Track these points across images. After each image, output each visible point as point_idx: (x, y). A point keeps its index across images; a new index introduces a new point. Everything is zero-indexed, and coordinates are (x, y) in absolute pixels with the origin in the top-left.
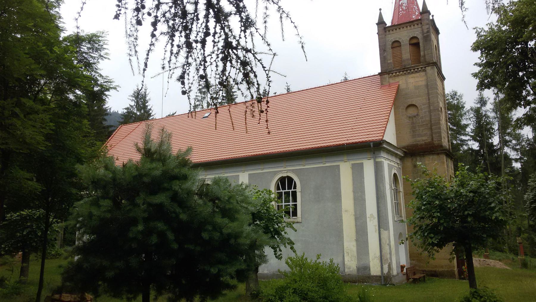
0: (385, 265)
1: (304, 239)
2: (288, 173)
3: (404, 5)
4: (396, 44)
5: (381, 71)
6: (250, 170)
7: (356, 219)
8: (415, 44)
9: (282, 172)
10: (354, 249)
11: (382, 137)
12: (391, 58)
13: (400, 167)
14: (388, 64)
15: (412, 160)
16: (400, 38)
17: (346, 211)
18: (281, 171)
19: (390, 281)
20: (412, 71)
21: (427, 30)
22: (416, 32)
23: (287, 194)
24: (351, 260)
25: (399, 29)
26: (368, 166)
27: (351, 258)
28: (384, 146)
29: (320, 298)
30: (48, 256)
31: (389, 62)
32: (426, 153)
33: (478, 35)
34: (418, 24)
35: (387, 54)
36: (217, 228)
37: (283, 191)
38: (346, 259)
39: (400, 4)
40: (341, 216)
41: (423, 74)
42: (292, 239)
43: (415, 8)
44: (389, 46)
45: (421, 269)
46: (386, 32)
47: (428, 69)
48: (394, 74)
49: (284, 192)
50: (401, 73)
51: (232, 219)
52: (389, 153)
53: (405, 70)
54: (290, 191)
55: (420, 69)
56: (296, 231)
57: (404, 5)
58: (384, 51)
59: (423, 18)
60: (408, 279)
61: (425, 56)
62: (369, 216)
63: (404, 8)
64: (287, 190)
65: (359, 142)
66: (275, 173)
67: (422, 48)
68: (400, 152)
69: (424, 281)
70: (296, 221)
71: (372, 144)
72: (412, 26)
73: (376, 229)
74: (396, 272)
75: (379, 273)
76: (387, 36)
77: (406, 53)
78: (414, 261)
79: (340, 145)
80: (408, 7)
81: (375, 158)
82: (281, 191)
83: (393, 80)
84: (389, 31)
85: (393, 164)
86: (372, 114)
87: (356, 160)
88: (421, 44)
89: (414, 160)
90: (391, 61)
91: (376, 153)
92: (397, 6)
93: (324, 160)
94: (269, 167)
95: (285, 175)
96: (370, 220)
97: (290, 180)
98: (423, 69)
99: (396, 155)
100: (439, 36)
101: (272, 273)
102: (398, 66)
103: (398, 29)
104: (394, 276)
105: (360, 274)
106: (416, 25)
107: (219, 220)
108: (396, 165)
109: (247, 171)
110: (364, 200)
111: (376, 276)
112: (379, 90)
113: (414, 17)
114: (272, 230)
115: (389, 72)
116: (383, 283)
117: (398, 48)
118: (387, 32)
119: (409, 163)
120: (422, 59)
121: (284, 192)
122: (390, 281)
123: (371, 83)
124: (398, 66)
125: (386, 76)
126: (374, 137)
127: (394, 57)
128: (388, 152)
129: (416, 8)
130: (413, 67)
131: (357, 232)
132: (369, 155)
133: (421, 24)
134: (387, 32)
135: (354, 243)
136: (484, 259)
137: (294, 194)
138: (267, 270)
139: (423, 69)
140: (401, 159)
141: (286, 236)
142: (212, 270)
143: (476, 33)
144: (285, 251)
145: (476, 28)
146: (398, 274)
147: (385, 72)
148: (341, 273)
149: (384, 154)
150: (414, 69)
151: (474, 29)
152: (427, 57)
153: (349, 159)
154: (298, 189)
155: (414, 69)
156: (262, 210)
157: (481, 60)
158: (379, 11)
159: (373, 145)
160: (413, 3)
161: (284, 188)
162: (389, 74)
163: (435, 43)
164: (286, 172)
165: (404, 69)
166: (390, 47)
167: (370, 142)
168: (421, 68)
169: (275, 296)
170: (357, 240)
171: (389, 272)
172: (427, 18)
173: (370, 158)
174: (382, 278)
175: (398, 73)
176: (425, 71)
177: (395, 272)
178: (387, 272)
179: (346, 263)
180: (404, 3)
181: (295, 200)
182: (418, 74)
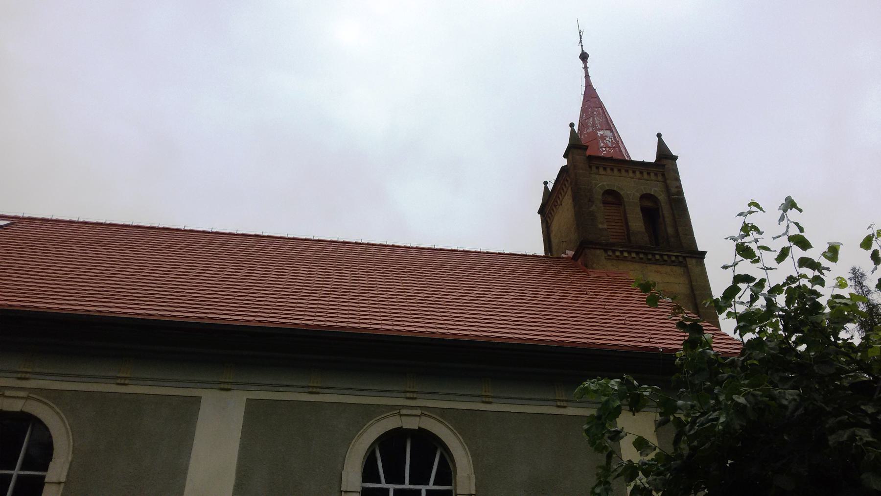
9: (404, 412)
31: (600, 226)
37: (392, 487)
48: (618, 254)
54: (424, 488)
63: (610, 144)
64: (407, 486)
66: (370, 413)
82: (383, 485)
83: (613, 265)
95: (411, 424)
98: (681, 259)
109: (246, 386)
125: (598, 252)
134: (594, 169)
150: (661, 255)
161: (395, 476)
162: (606, 251)
164: (418, 412)
168: (677, 257)
175: (626, 254)
182: (668, 269)
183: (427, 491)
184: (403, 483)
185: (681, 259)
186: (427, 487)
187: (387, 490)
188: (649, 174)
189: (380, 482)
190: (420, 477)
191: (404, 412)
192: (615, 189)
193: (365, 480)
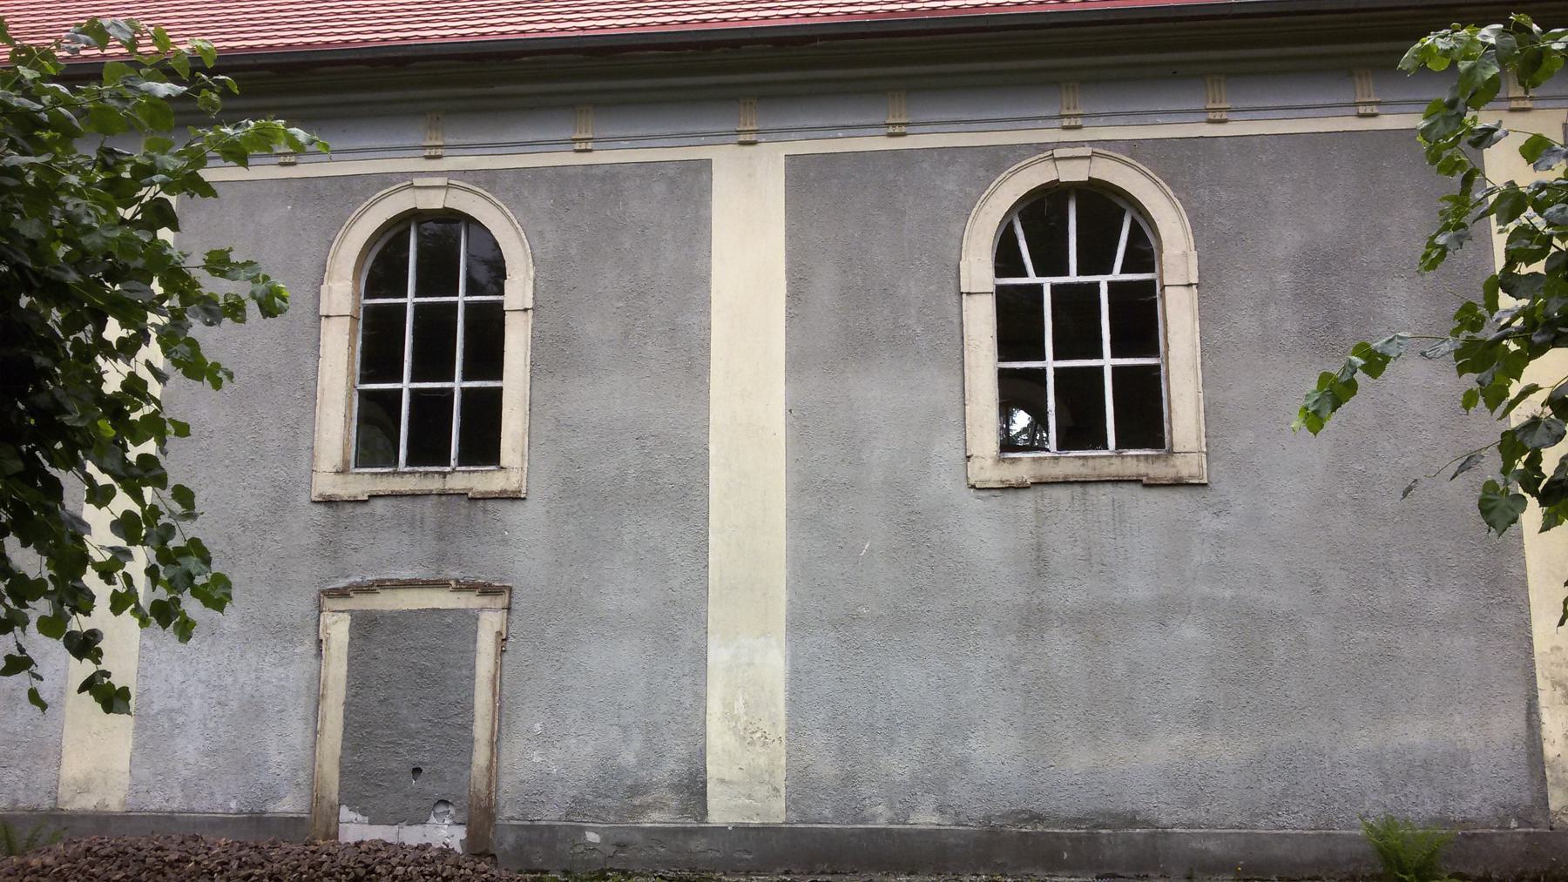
1: (1228, 593)
2: (1096, 160)
6: (801, 129)
9: (1058, 153)
18: (1040, 147)
37: (1047, 282)
49: (1054, 287)
54: (1103, 281)
64: (1073, 277)
66: (998, 161)
70: (1160, 471)
82: (1032, 279)
94: (951, 117)
101: (973, 827)
121: (1054, 287)
138: (941, 809)
148: (1519, 818)
161: (1051, 262)
164: (1087, 151)
179: (1550, 751)
183: (1110, 284)
184: (1066, 273)
186: (1110, 278)
187: (1039, 287)
189: (1025, 275)
190: (1096, 260)
191: (1058, 153)
193: (999, 273)
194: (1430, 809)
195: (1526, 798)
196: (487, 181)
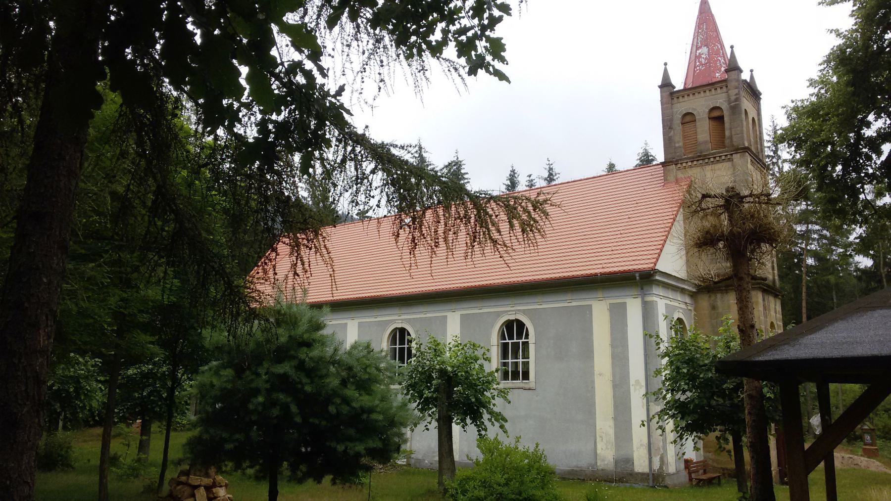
0: (655, 456)
3: (703, 56)
4: (688, 119)
5: (665, 159)
7: (615, 386)
8: (717, 118)
10: (611, 432)
11: (653, 265)
12: (681, 140)
13: (689, 308)
14: (676, 148)
15: (710, 297)
16: (695, 110)
17: (600, 375)
19: (662, 481)
20: (712, 160)
21: (735, 97)
22: (719, 99)
23: (516, 346)
24: (607, 448)
25: (694, 94)
26: (634, 307)
27: (606, 445)
28: (657, 278)
29: (513, 494)
30: (178, 427)
31: (677, 145)
32: (731, 288)
33: (788, 118)
34: (721, 88)
35: (674, 132)
36: (346, 401)
37: (510, 341)
38: (599, 446)
39: (698, 54)
40: (593, 382)
41: (727, 165)
42: (505, 414)
43: (720, 61)
44: (678, 118)
45: (719, 466)
46: (673, 99)
47: (737, 157)
48: (684, 165)
50: (695, 163)
51: (369, 392)
52: (668, 288)
53: (701, 158)
54: (521, 341)
55: (723, 158)
56: (510, 402)
57: (703, 56)
58: (670, 128)
59: (731, 78)
60: (691, 479)
61: (731, 137)
62: (634, 384)
63: (703, 61)
64: (515, 341)
65: (620, 272)
66: (499, 314)
67: (727, 125)
68: (687, 285)
69: (719, 484)
70: (527, 386)
71: (637, 275)
72: (713, 90)
73: (643, 402)
74: (674, 468)
75: (647, 470)
76: (675, 106)
77: (704, 131)
78: (710, 454)
79: (591, 275)
80: (709, 60)
81: (643, 295)
82: (507, 341)
84: (678, 98)
85: (676, 304)
86: (644, 229)
87: (616, 297)
88: (725, 119)
89: (713, 298)
90: (681, 144)
91: (645, 288)
92: (693, 58)
93: (569, 296)
95: (512, 318)
96: (635, 390)
97: (521, 325)
99: (683, 291)
100: (762, 101)
102: (691, 152)
103: (691, 95)
104: (669, 475)
105: (619, 470)
106: (719, 89)
107: (351, 392)
108: (684, 306)
110: (627, 359)
111: (643, 474)
112: (660, 188)
113: (717, 75)
114: (473, 400)
115: (677, 161)
116: (651, 484)
117: (691, 125)
118: (675, 99)
119: (705, 302)
120: (727, 142)
122: (662, 481)
123: (651, 177)
124: (691, 152)
125: (671, 167)
126: (643, 265)
127: (684, 137)
128: (668, 286)
129: (723, 61)
130: (712, 154)
131: (616, 406)
132: (635, 291)
133: (727, 87)
134: (675, 99)
135: (611, 423)
136: (851, 456)
137: (526, 344)
139: (729, 157)
140: (693, 295)
141: (495, 409)
142: (338, 447)
143: (786, 113)
144: (493, 431)
145: (785, 107)
146: (678, 472)
147: (671, 162)
149: (657, 290)
150: (715, 158)
151: (784, 108)
152: (734, 140)
153: (606, 296)
154: (532, 340)
155: (715, 158)
156: (459, 372)
157: (791, 155)
158: (664, 66)
159: (640, 276)
160: (717, 53)
161: (511, 338)
162: (676, 164)
163: (752, 114)
164: (514, 313)
165: (699, 156)
166: (679, 122)
167: (635, 271)
169: (456, 489)
170: (615, 419)
171: (661, 467)
172: (735, 79)
173: (637, 296)
174: (651, 476)
175: (690, 164)
176: (731, 160)
177: (672, 469)
178: (658, 468)
179: (598, 452)
180: (703, 54)
181: (526, 355)
182: (719, 165)
185: (729, 157)
188: (716, 89)
192: (690, 111)
194: (575, 464)
195: (593, 462)
196: (409, 321)
